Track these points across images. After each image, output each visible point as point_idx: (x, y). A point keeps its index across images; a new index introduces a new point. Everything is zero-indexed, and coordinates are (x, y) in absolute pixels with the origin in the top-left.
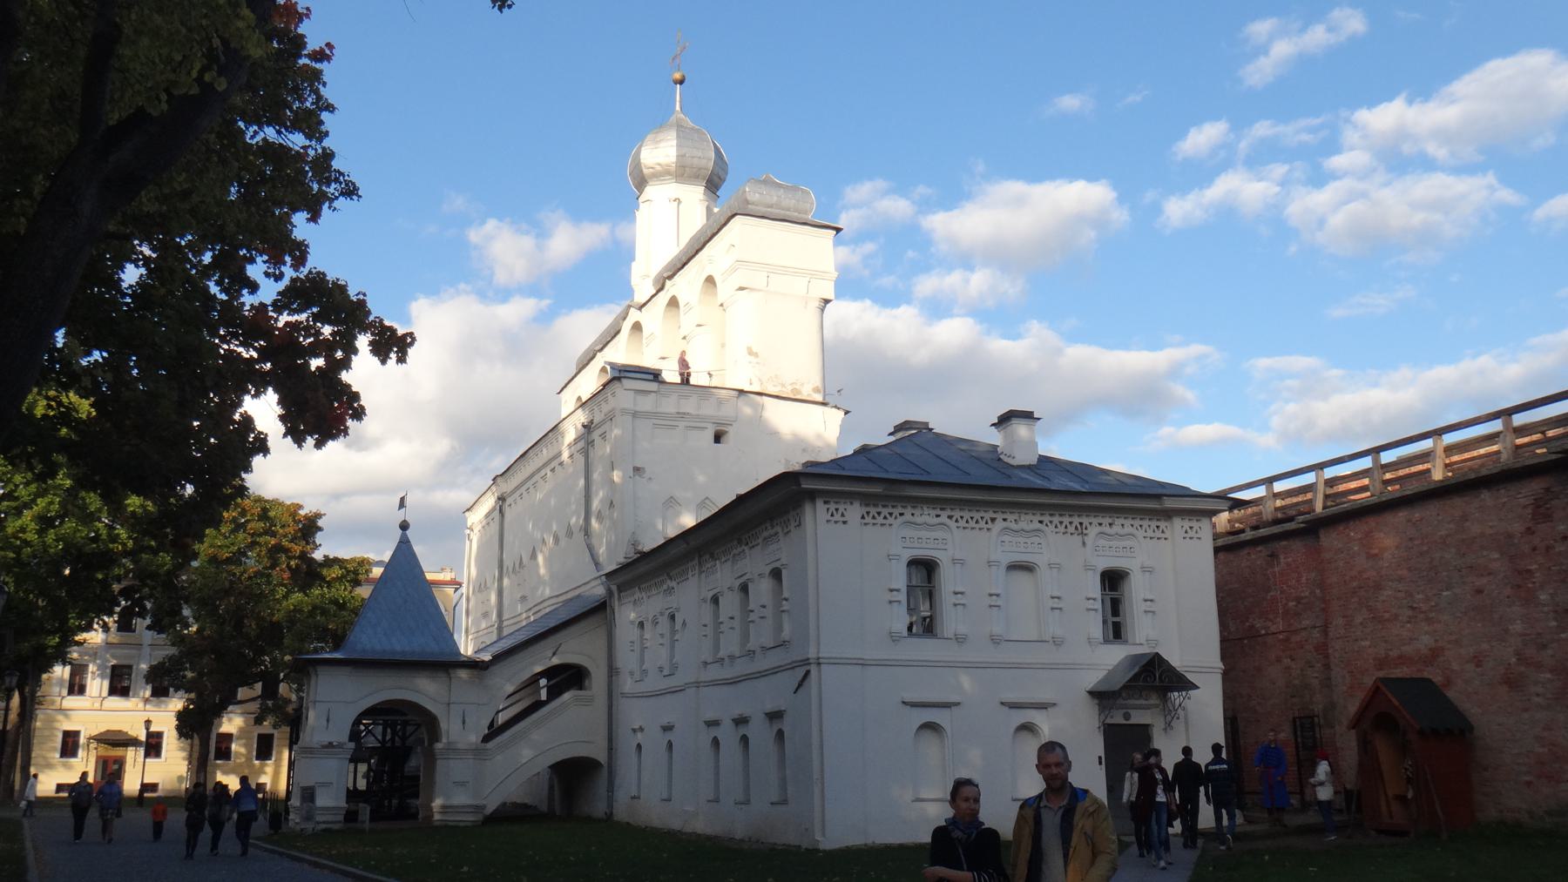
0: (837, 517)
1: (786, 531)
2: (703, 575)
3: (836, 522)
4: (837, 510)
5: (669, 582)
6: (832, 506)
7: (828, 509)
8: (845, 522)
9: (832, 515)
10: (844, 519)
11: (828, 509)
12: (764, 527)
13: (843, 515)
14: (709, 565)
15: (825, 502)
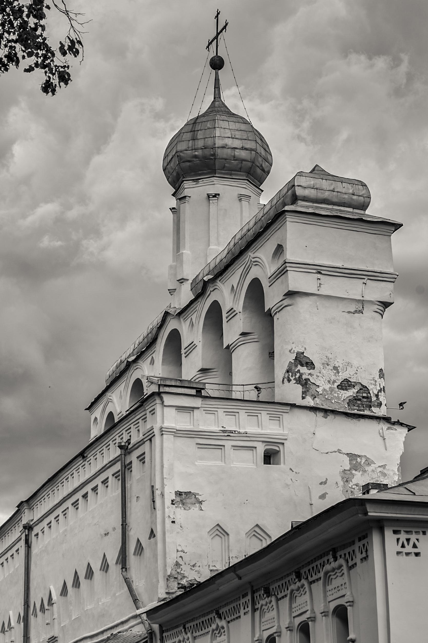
0: (409, 549)
1: (350, 563)
2: (257, 614)
3: (408, 554)
4: (408, 540)
5: (218, 620)
6: (403, 537)
7: (398, 540)
8: (417, 554)
9: (403, 546)
10: (416, 550)
11: (398, 540)
12: (325, 559)
13: (415, 546)
14: (263, 602)
15: (395, 532)
